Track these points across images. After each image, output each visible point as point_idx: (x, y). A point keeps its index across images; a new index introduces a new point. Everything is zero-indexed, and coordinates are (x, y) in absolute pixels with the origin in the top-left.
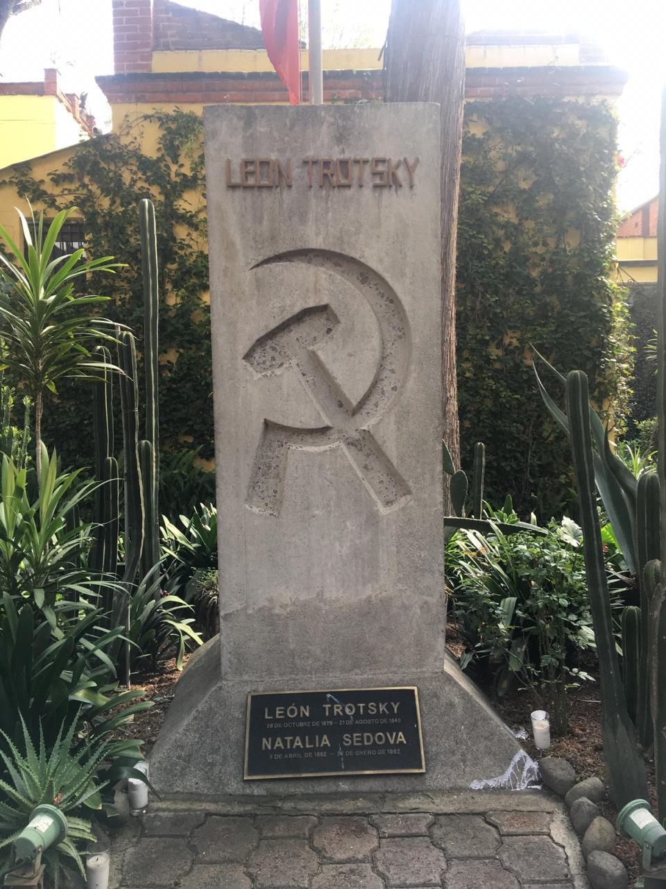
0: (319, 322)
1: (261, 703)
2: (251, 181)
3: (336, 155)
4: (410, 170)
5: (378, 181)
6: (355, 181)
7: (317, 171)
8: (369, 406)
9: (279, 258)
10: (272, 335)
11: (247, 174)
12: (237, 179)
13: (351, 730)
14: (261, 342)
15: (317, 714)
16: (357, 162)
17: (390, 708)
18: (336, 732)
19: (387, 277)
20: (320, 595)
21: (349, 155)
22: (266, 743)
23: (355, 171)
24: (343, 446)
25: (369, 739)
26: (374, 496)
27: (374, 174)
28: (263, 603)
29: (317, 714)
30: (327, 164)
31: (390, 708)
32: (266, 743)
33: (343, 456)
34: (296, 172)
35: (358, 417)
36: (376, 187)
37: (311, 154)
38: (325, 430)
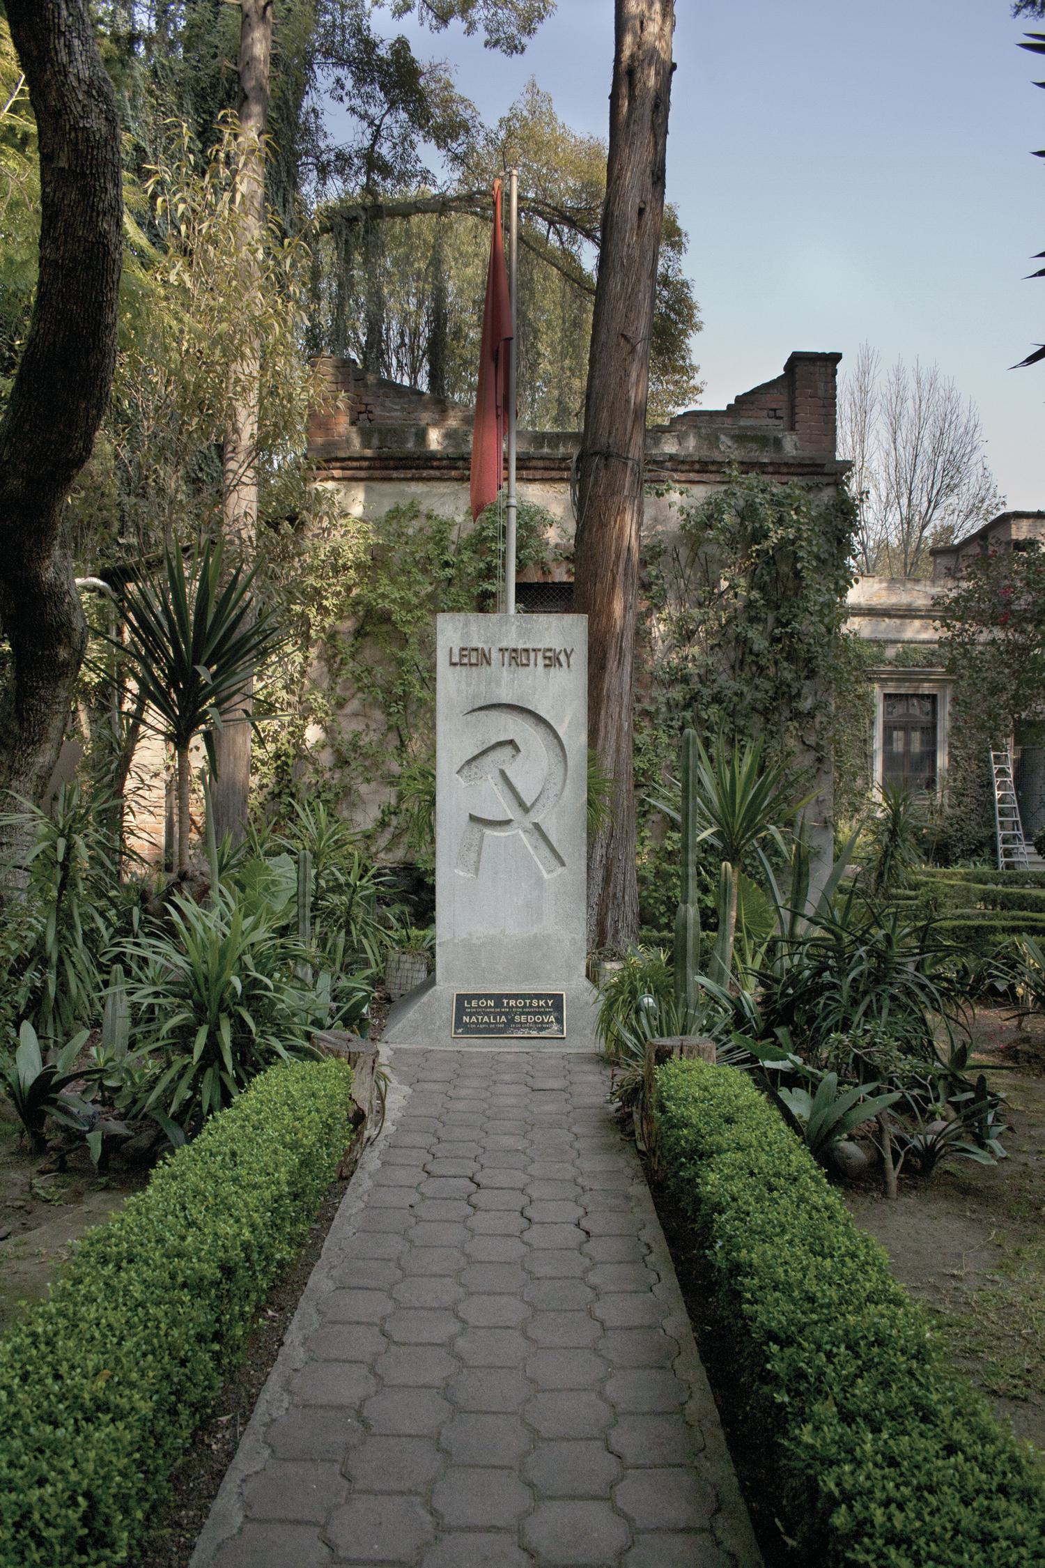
0: (508, 750)
1: (461, 998)
2: (465, 660)
3: (520, 646)
4: (568, 656)
5: (547, 662)
6: (532, 662)
7: (506, 654)
8: (539, 805)
9: (481, 709)
10: (475, 758)
11: (462, 656)
12: (456, 659)
13: (522, 1014)
14: (469, 762)
15: (499, 1004)
16: (534, 650)
17: (546, 1003)
18: (510, 1013)
19: (552, 723)
20: (503, 932)
21: (528, 646)
22: (466, 1019)
23: (532, 655)
24: (521, 832)
25: (531, 1019)
26: (541, 867)
27: (545, 658)
28: (464, 936)
29: (499, 1004)
30: (515, 650)
31: (546, 1003)
32: (466, 1019)
33: (521, 839)
34: (495, 656)
35: (531, 813)
36: (546, 666)
37: (504, 645)
38: (508, 822)
